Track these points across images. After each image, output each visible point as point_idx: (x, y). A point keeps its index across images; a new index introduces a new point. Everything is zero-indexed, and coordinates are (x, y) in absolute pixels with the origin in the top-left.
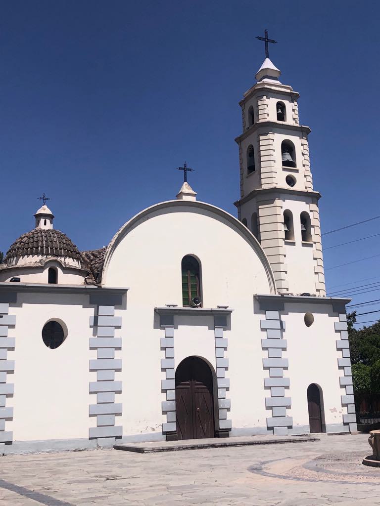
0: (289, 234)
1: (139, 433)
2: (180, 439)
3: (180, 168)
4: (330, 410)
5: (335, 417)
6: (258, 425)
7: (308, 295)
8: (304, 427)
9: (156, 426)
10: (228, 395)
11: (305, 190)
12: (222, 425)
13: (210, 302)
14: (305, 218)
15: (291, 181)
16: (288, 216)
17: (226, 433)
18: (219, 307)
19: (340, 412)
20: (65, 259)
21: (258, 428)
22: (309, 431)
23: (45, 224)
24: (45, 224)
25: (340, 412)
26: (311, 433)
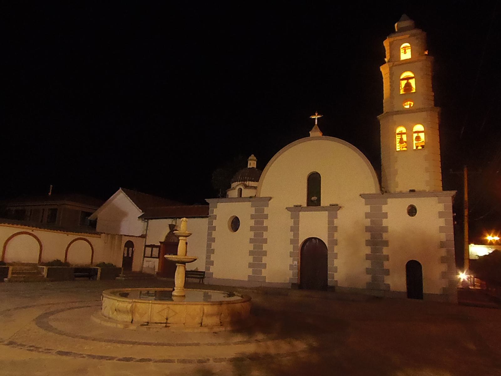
12: (330, 284)
13: (325, 201)
23: (250, 165)
24: (250, 165)
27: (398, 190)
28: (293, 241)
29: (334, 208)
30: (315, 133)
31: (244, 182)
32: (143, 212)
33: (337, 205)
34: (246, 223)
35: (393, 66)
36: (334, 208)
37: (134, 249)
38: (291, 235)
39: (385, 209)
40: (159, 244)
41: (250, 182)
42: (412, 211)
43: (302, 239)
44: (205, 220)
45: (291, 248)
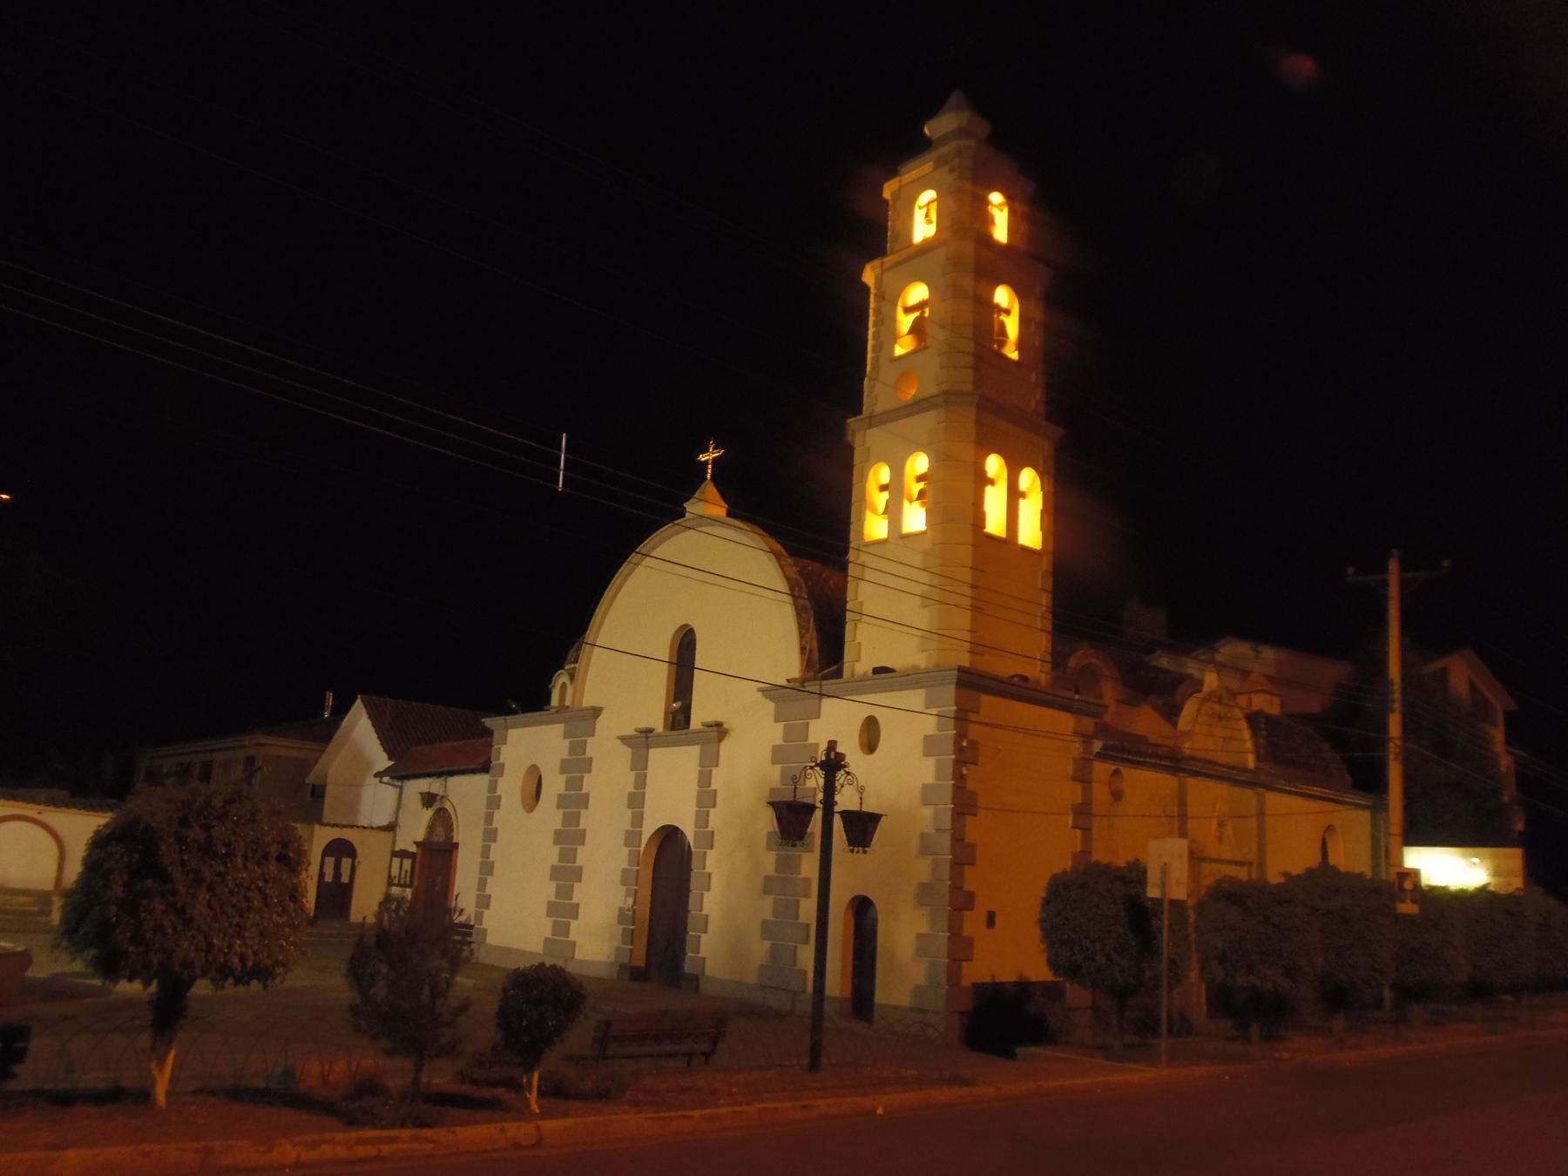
17: (695, 980)
28: (631, 838)
30: (707, 504)
32: (390, 759)
34: (554, 785)
35: (883, 272)
36: (718, 730)
37: (357, 861)
40: (413, 849)
43: (648, 829)
44: (482, 780)
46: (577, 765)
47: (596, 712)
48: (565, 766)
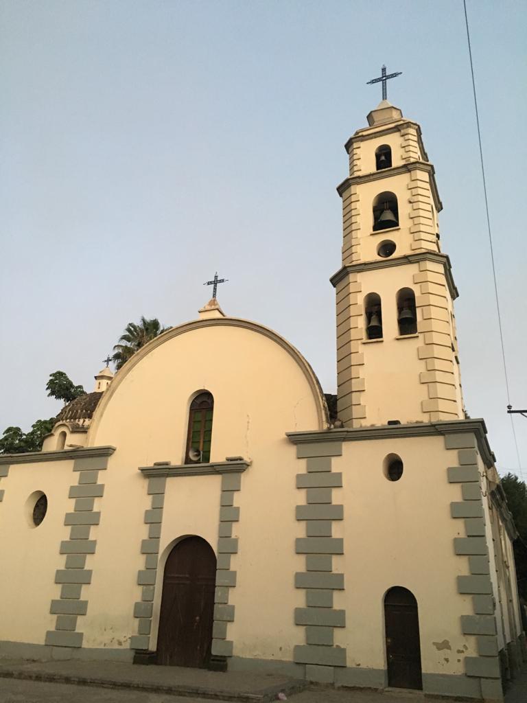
0: (375, 332)
1: (103, 647)
2: (166, 665)
3: (209, 283)
4: (434, 643)
5: (447, 660)
6: (279, 656)
7: (397, 422)
8: (371, 672)
9: (125, 639)
10: (234, 597)
11: (409, 252)
12: (216, 650)
13: (218, 455)
14: (406, 300)
15: (387, 248)
16: (373, 305)
17: (220, 664)
18: (228, 460)
19: (459, 652)
20: (84, 421)
21: (281, 661)
22: (383, 680)
25: (459, 652)
26: (390, 685)
27: (366, 424)
28: (148, 548)
29: (235, 467)
31: (75, 419)
33: (241, 459)
34: (60, 506)
38: (144, 532)
39: (336, 465)
41: (87, 420)
42: (394, 468)
43: (167, 538)
45: (140, 563)
46: (87, 493)
47: (106, 452)
48: (73, 493)
